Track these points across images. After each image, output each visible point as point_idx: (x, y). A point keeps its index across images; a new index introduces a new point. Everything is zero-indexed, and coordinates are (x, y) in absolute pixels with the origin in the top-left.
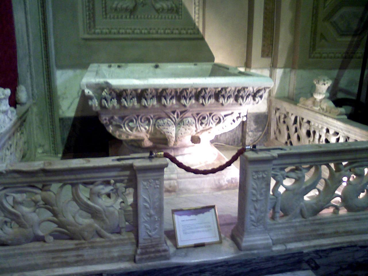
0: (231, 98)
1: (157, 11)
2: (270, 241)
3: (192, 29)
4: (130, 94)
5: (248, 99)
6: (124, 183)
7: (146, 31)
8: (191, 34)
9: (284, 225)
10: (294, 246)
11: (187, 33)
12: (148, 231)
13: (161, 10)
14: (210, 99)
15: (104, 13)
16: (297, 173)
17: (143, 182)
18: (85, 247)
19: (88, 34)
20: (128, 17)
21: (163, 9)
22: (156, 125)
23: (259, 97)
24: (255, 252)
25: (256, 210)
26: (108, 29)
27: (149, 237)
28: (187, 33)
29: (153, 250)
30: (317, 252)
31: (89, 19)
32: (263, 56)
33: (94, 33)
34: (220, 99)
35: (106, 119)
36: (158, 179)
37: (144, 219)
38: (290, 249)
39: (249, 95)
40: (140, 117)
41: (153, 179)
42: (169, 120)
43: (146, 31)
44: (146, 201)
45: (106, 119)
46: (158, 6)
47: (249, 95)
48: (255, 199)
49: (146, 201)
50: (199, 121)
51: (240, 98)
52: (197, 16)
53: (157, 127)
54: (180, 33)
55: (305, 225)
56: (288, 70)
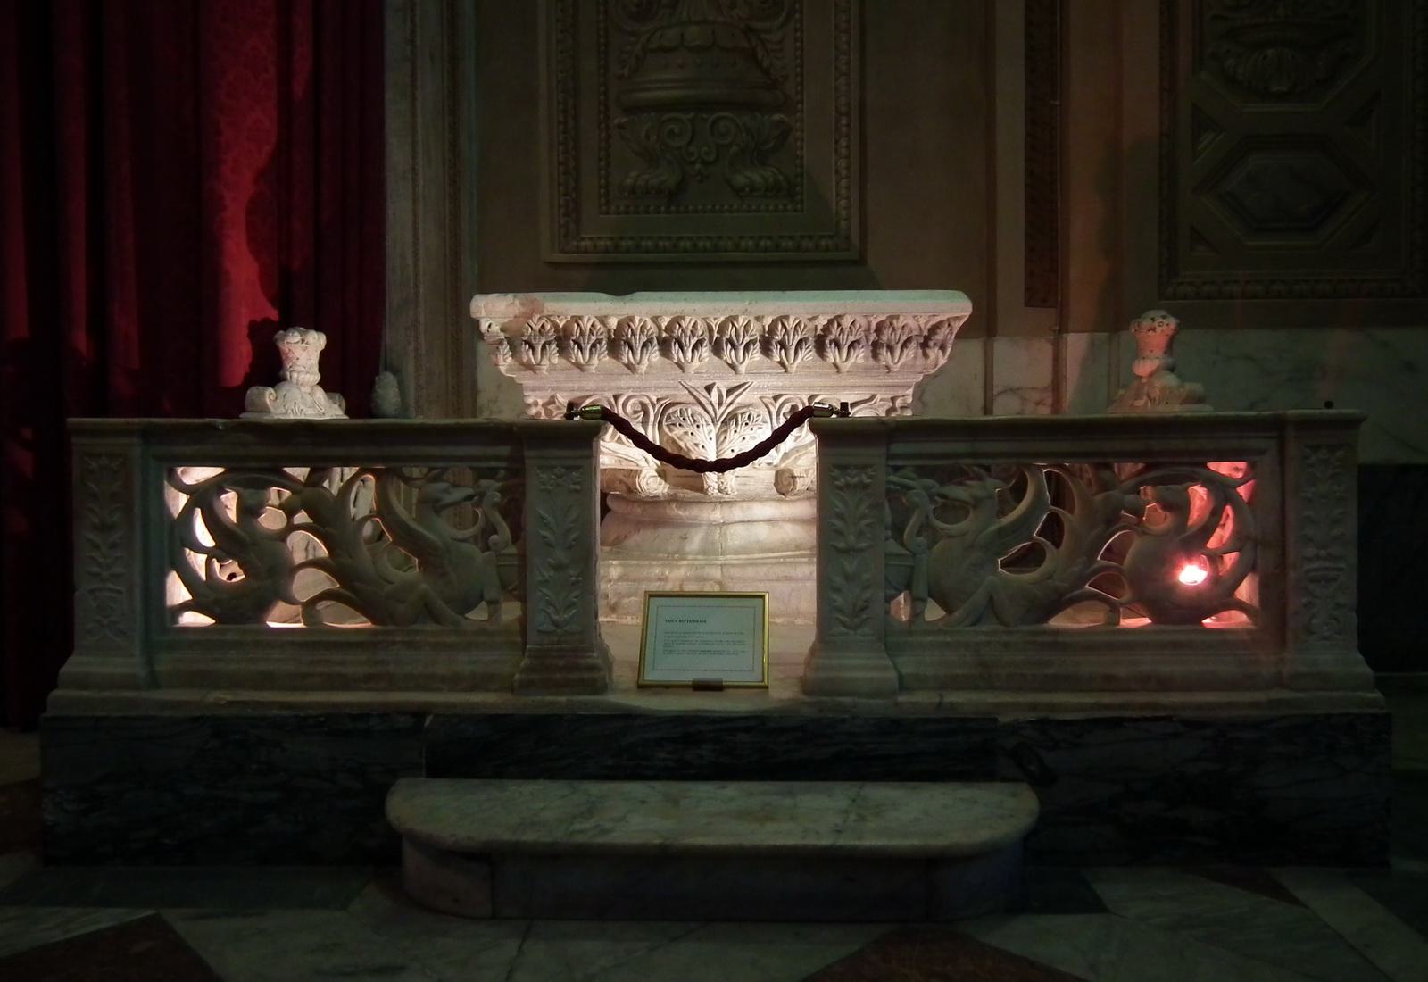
0: (857, 351)
1: (738, 192)
2: (892, 675)
3: (831, 237)
4: (591, 332)
5: (905, 351)
6: (498, 481)
7: (708, 244)
8: (827, 249)
9: (940, 638)
10: (964, 700)
11: (817, 247)
12: (551, 610)
13: (747, 189)
14: (801, 349)
15: (603, 200)
16: (970, 486)
17: (538, 471)
18: (394, 643)
19: (563, 251)
20: (663, 209)
21: (753, 189)
22: (664, 423)
23: (936, 349)
24: (847, 700)
25: (847, 577)
26: (611, 239)
27: (553, 628)
28: (817, 247)
29: (561, 663)
30: (1043, 724)
31: (567, 215)
32: (1029, 302)
33: (578, 250)
34: (829, 350)
35: (536, 404)
36: (577, 468)
37: (543, 576)
38: (952, 706)
39: (909, 340)
40: (621, 401)
41: (563, 467)
42: (700, 410)
43: (708, 244)
44: (546, 526)
45: (536, 404)
46: (740, 180)
47: (909, 340)
48: (841, 545)
49: (546, 526)
50: (781, 416)
51: (885, 349)
52: (843, 203)
53: (666, 430)
54: (798, 249)
55: (1006, 645)
56: (1104, 335)
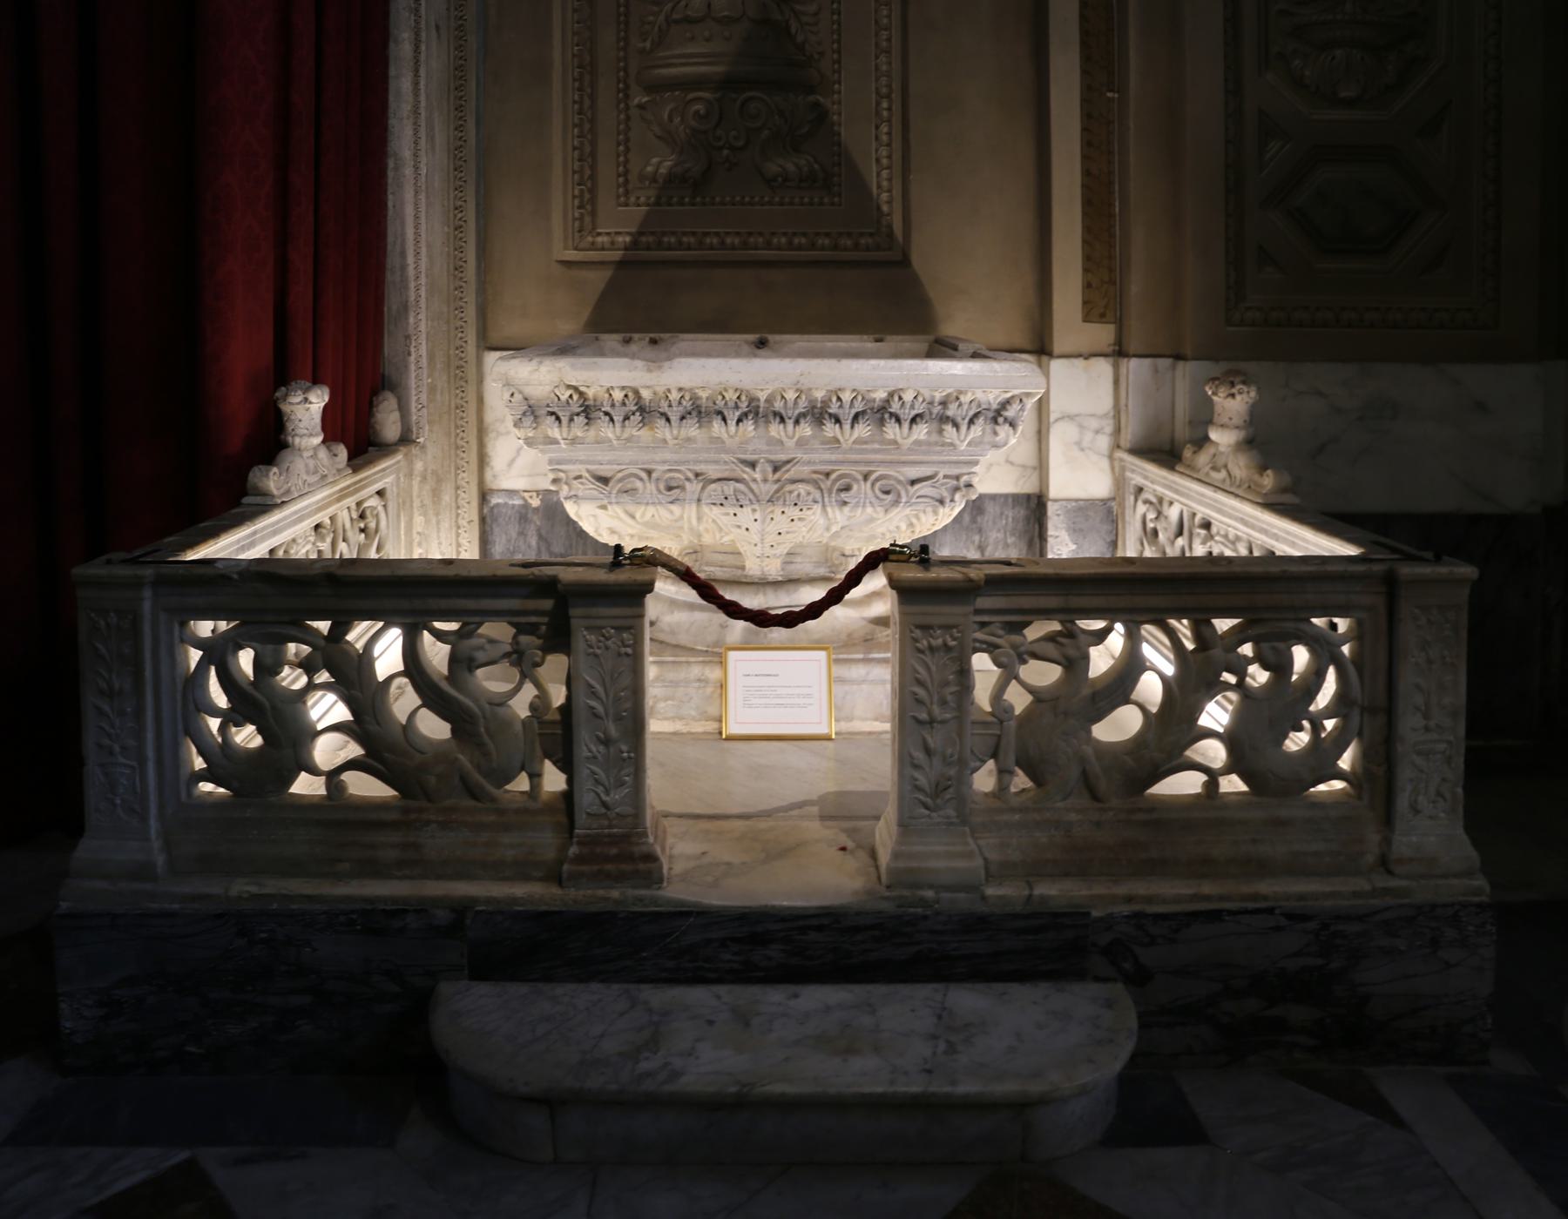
2: (979, 862)
3: (871, 235)
5: (973, 428)
7: (737, 241)
11: (856, 246)
12: (600, 789)
13: (780, 179)
19: (576, 249)
37: (590, 751)
38: (1044, 899)
39: (976, 415)
43: (737, 241)
44: (594, 695)
46: (772, 168)
49: (594, 695)
54: (835, 247)
